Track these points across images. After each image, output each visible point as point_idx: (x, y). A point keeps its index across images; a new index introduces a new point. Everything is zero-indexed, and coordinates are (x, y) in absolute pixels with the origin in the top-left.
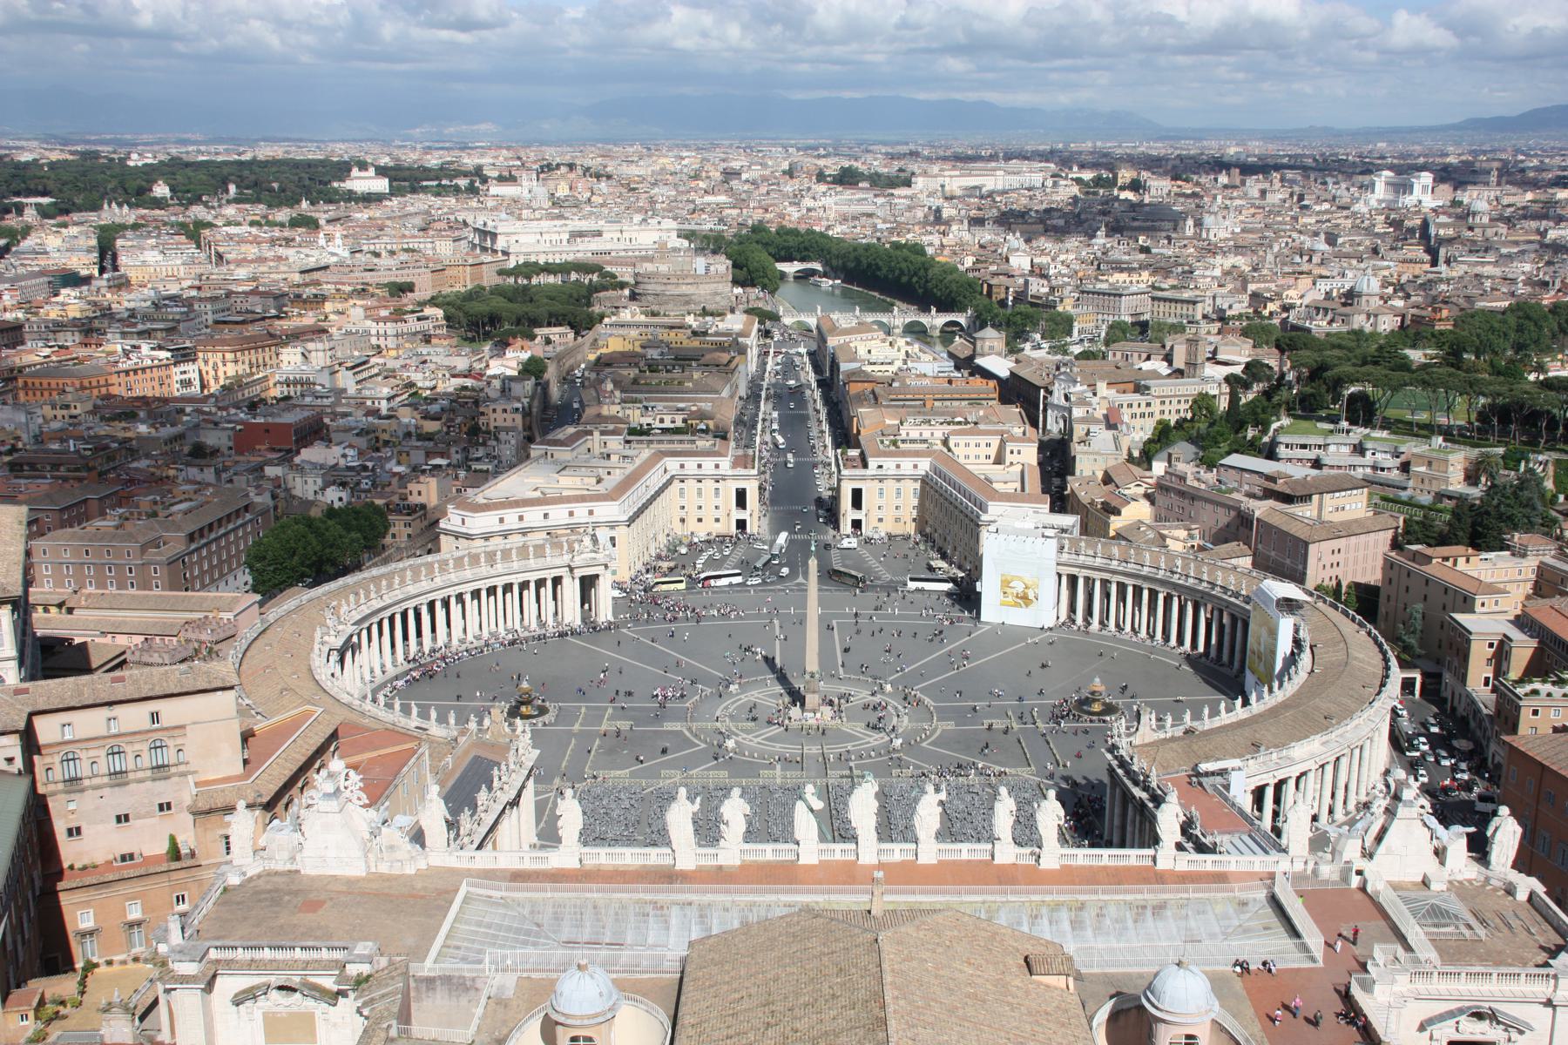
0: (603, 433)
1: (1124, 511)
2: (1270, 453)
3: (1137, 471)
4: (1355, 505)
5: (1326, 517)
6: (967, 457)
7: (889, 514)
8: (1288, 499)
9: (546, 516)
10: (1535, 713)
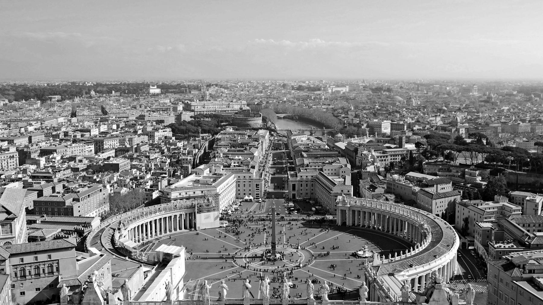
0: (215, 167)
1: (376, 190)
2: (422, 173)
3: (381, 178)
4: (448, 188)
5: (439, 191)
6: (329, 174)
7: (304, 192)
8: (427, 186)
9: (194, 193)
10: (500, 253)
